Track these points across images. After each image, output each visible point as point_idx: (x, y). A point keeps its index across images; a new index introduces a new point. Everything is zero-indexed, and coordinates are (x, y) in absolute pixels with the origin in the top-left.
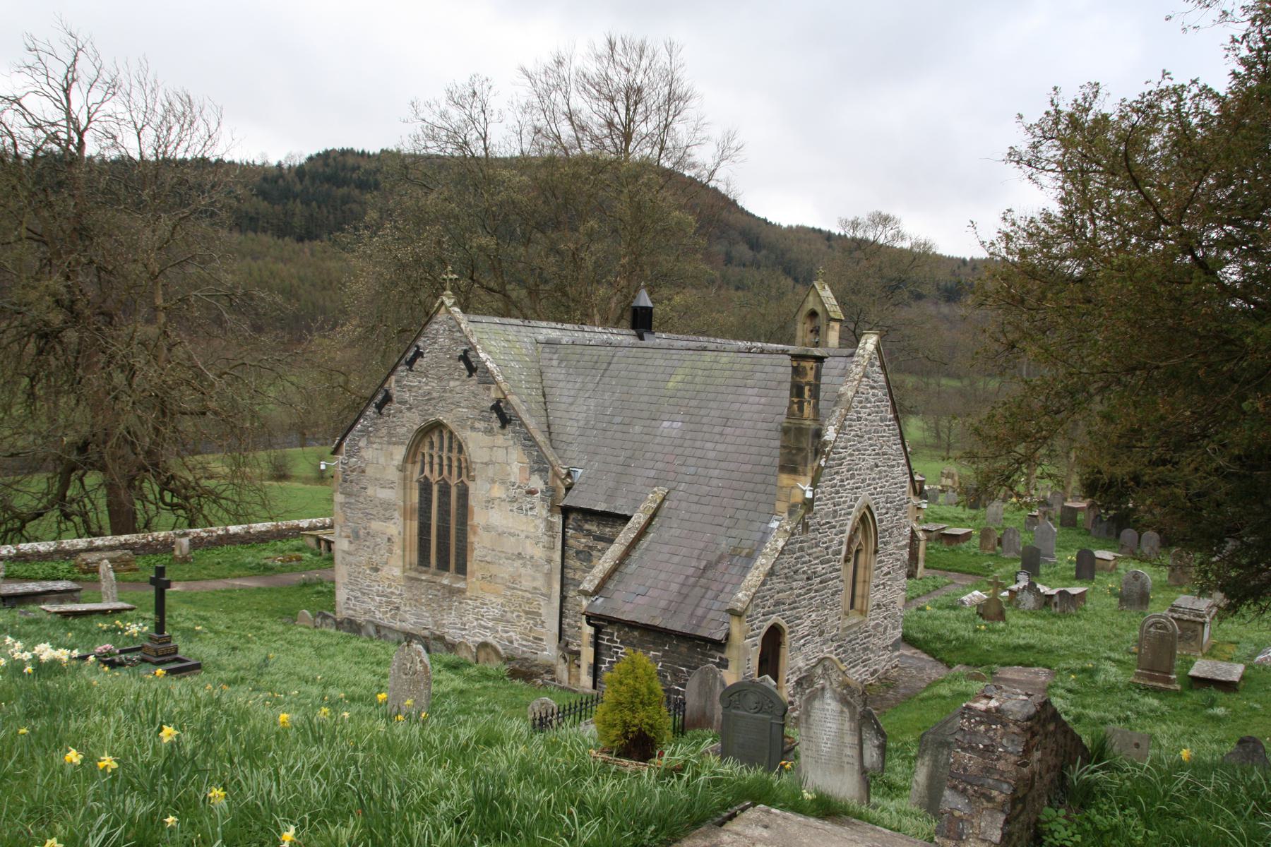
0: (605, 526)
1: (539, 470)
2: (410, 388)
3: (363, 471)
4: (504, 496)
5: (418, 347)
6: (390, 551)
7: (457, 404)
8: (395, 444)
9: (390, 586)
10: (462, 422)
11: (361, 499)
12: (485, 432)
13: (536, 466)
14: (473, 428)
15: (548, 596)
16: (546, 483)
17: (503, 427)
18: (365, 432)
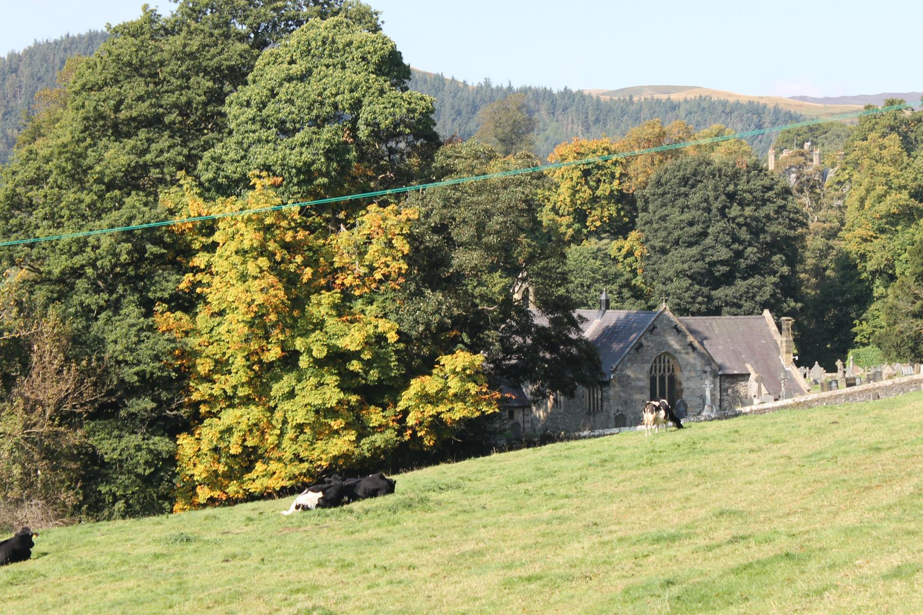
18: (630, 360)
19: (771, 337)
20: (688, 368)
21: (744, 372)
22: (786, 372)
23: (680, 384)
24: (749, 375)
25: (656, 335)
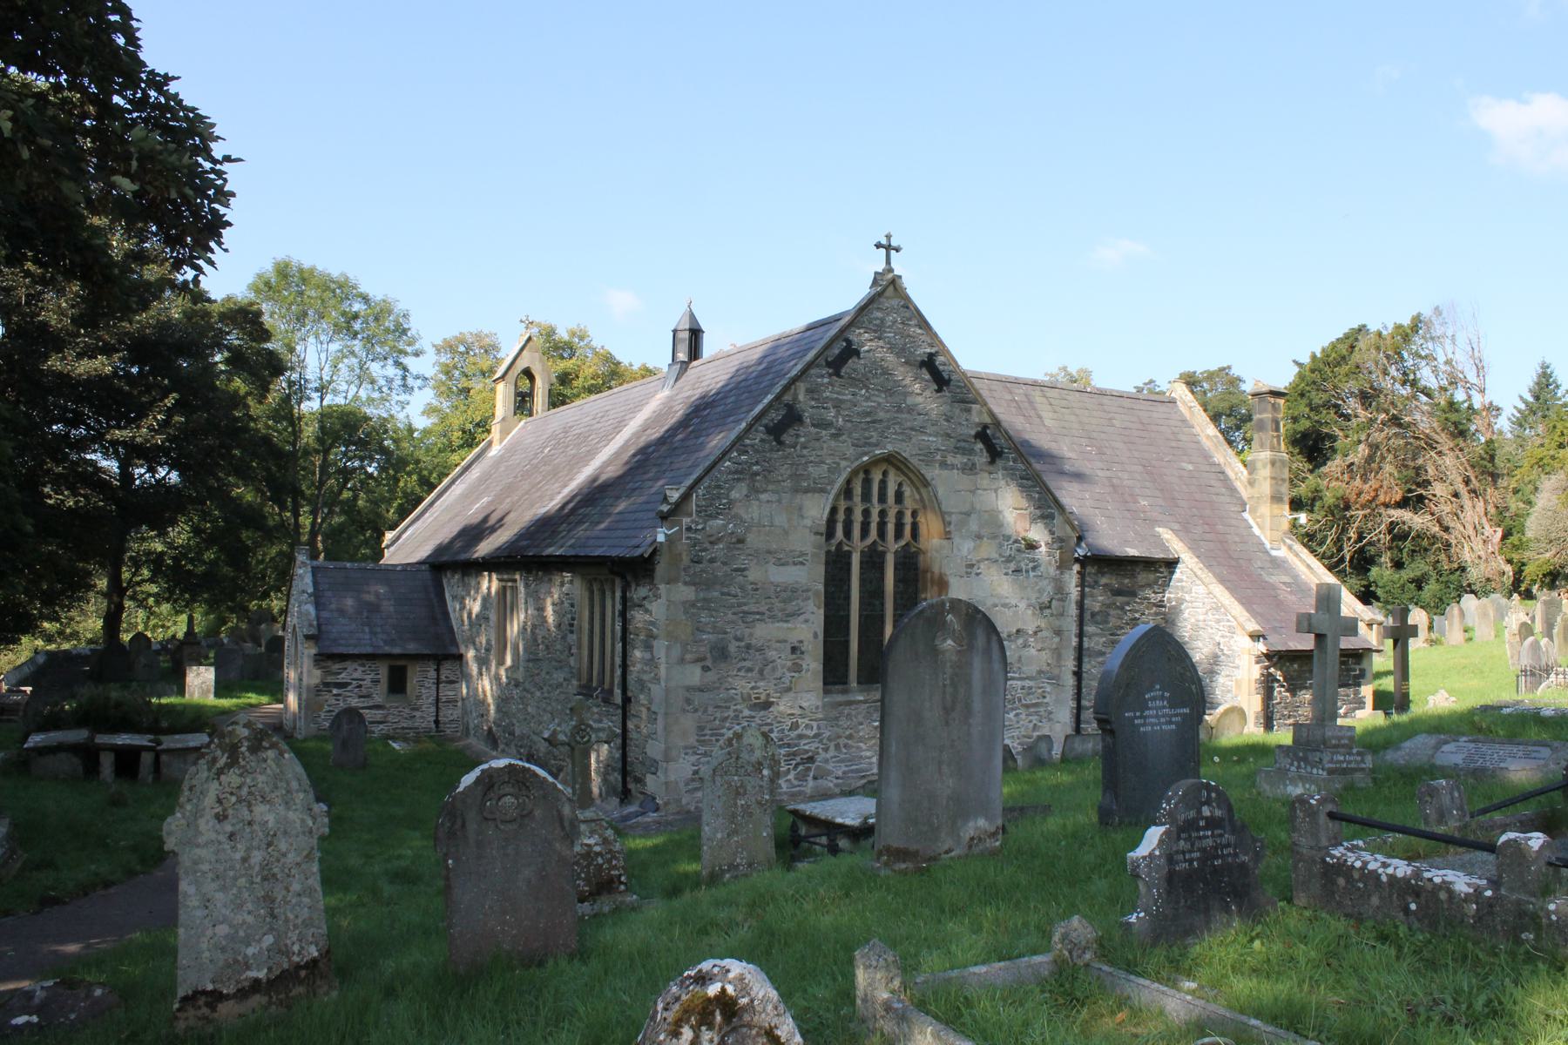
0: (1125, 576)
1: (1043, 517)
2: (838, 405)
3: (741, 541)
4: (995, 556)
5: (849, 342)
6: (797, 668)
7: (921, 430)
8: (807, 491)
9: (795, 726)
10: (928, 456)
11: (733, 590)
12: (963, 470)
13: (1038, 512)
14: (944, 465)
15: (1055, 680)
16: (1052, 533)
17: (992, 462)
18: (740, 473)
19: (1206, 456)
20: (974, 526)
21: (1158, 554)
22: (1277, 564)
23: (942, 584)
24: (1171, 564)
25: (854, 381)
